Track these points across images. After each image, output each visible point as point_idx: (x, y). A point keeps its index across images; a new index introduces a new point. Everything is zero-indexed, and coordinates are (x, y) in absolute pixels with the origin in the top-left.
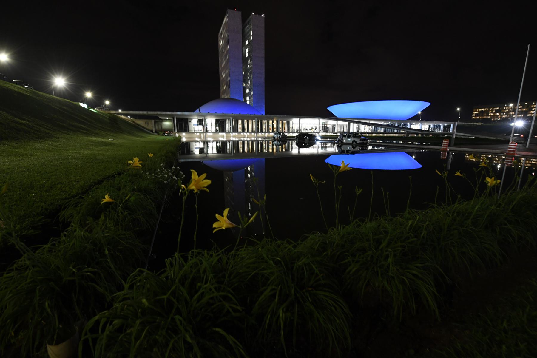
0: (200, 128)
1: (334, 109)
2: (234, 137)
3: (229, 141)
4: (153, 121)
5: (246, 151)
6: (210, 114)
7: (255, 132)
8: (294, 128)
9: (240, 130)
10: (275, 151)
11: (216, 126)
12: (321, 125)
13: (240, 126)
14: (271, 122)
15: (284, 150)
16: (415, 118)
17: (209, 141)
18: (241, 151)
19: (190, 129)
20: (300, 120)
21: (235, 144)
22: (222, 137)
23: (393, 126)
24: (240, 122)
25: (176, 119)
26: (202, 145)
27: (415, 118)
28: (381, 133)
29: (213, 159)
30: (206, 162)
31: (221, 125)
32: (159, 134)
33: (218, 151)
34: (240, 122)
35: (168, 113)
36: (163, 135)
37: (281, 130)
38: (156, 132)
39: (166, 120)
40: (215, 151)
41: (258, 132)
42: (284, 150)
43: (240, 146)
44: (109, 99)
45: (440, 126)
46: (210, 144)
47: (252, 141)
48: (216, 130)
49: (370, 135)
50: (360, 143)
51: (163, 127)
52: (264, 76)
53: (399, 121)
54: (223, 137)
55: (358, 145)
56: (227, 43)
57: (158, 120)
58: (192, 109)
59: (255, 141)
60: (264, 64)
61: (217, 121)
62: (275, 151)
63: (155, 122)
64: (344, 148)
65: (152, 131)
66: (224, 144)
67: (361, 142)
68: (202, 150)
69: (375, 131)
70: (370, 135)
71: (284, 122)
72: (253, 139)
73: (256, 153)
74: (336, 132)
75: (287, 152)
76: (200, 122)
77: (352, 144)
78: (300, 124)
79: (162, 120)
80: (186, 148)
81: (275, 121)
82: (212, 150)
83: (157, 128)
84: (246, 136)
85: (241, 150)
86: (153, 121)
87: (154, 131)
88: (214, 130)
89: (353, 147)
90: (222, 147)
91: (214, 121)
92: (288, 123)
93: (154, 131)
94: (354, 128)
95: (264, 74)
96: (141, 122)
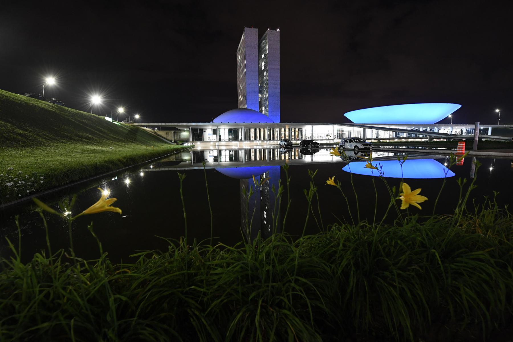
0: (215, 137)
1: (350, 115)
2: (246, 145)
3: (241, 149)
4: (173, 132)
5: (258, 159)
6: (222, 123)
7: (267, 141)
8: (307, 135)
9: (251, 139)
11: (229, 136)
13: (252, 135)
14: (283, 130)
15: (297, 158)
17: (223, 150)
18: (253, 158)
19: (205, 138)
20: (312, 127)
21: (248, 152)
22: (235, 145)
23: (419, 131)
24: (252, 130)
25: (192, 129)
26: (215, 154)
27: (445, 122)
28: (403, 138)
29: (225, 167)
30: (218, 169)
31: (234, 134)
32: (177, 144)
33: (231, 160)
34: (252, 130)
35: (184, 124)
37: (293, 137)
38: (175, 142)
40: (228, 159)
42: (297, 158)
43: (253, 154)
44: (139, 113)
46: (223, 152)
47: (264, 150)
48: (229, 139)
49: (391, 141)
50: (362, 149)
51: (182, 137)
52: (279, 86)
53: (424, 125)
55: (360, 150)
56: (245, 58)
57: (177, 131)
58: (209, 120)
59: (267, 148)
60: (279, 75)
61: (230, 130)
62: (287, 158)
63: (174, 133)
64: (348, 154)
65: (171, 141)
66: (237, 152)
67: (363, 147)
68: (215, 159)
69: (397, 136)
70: (391, 141)
71: (297, 129)
72: (265, 147)
73: (268, 161)
75: (300, 160)
76: (214, 132)
77: (354, 150)
78: (312, 131)
79: (181, 131)
80: (199, 156)
81: (287, 130)
82: (225, 159)
83: (176, 138)
84: (258, 145)
85: (253, 158)
87: (173, 141)
88: (227, 139)
89: (355, 153)
90: (235, 156)
91: (227, 131)
92: (301, 130)
93: (173, 141)
95: (279, 84)
96: (162, 133)
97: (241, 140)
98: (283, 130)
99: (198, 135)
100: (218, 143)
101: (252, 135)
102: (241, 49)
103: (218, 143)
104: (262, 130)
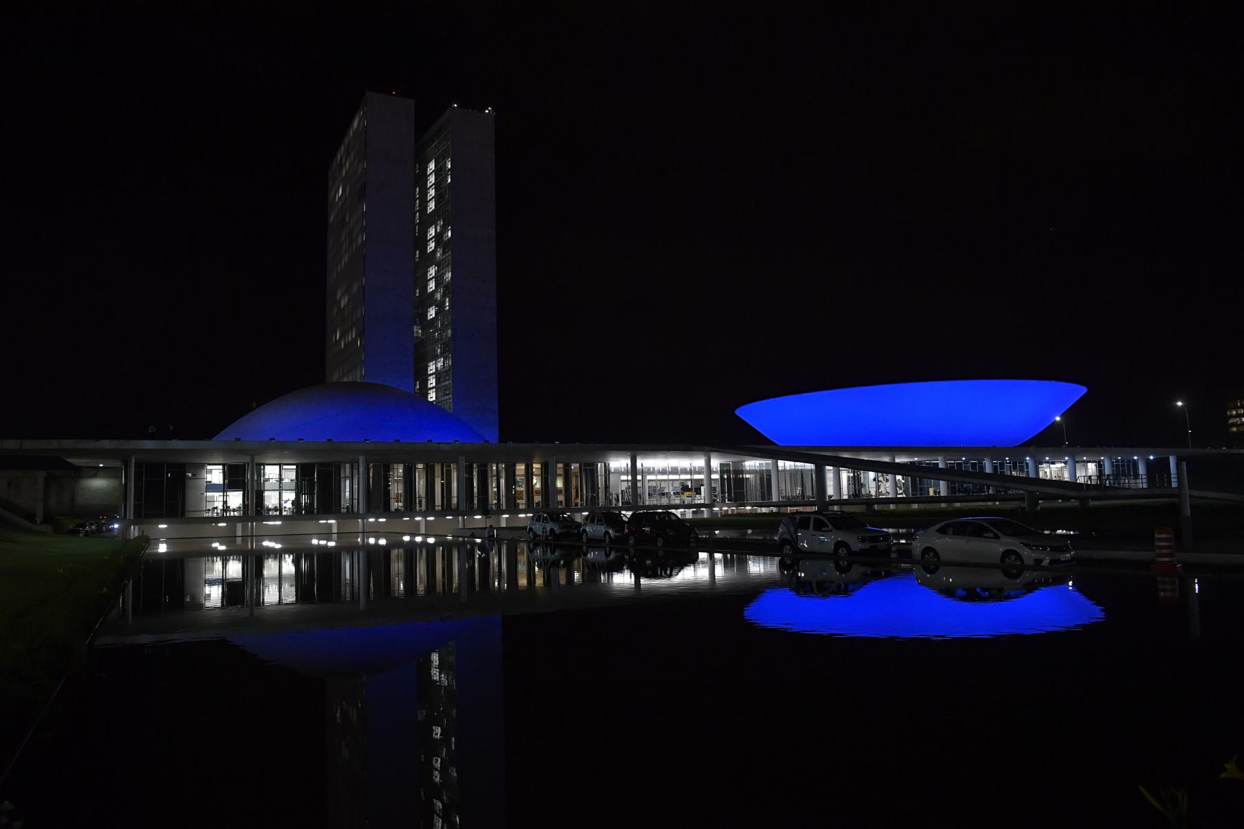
3: (352, 549)
4: (41, 475)
5: (421, 588)
6: (278, 448)
7: (456, 512)
9: (395, 505)
10: (539, 582)
12: (715, 476)
13: (396, 489)
14: (521, 468)
16: (1049, 441)
19: (190, 505)
21: (377, 560)
23: (979, 473)
26: (235, 569)
28: (938, 499)
29: (281, 618)
31: (319, 489)
35: (106, 444)
36: (74, 532)
37: (561, 498)
38: (48, 519)
39: (95, 472)
40: (290, 595)
41: (471, 512)
43: (397, 567)
45: (1135, 463)
47: (448, 548)
49: (902, 507)
53: (995, 451)
54: (328, 537)
57: (65, 473)
59: (459, 546)
61: (304, 472)
62: (539, 582)
65: (31, 517)
66: (328, 560)
68: (232, 590)
69: (917, 493)
70: (902, 507)
74: (775, 499)
76: (234, 480)
80: (174, 579)
81: (536, 466)
82: (278, 586)
84: (421, 532)
86: (41, 475)
90: (318, 577)
91: (290, 474)
92: (589, 471)
94: (838, 483)
97: (350, 509)
98: (521, 468)
99: (166, 493)
100: (250, 529)
101: (396, 489)
102: (346, 162)
103: (250, 529)
104: (438, 468)
